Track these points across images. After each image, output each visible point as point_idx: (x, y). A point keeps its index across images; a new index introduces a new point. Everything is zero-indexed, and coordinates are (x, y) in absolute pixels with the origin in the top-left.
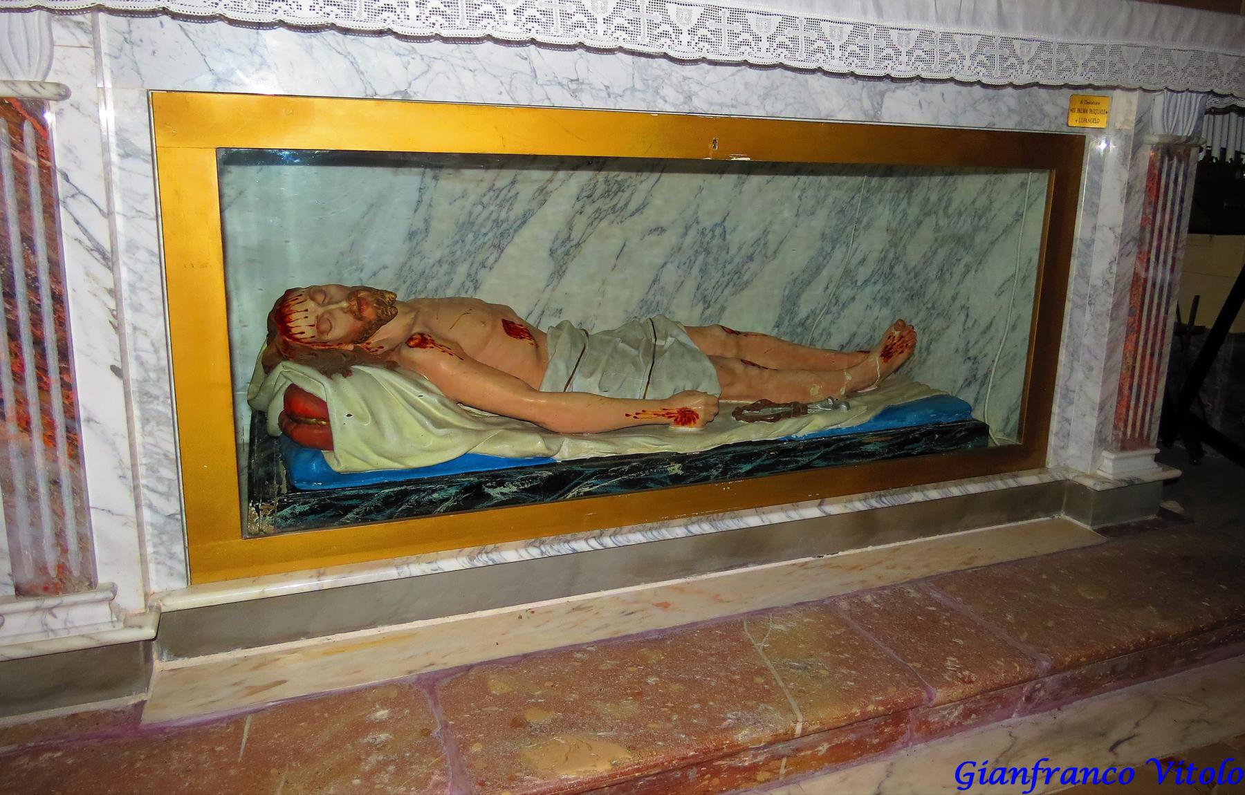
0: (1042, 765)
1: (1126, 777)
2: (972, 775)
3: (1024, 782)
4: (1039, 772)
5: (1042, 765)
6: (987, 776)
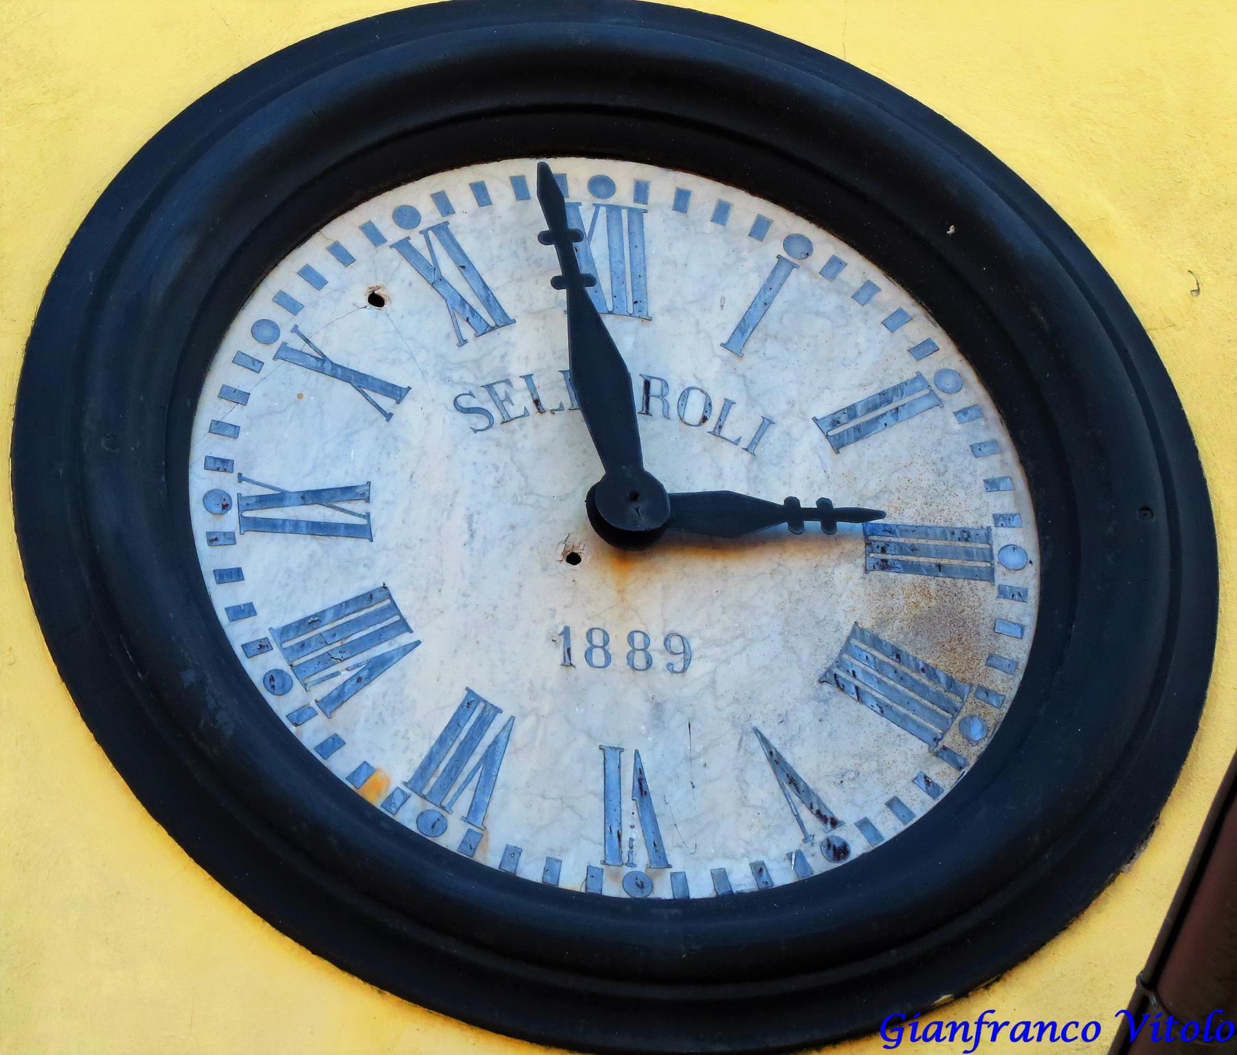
0: (989, 1018)
1: (1091, 1031)
3: (965, 1039)
4: (984, 1027)
5: (989, 1018)
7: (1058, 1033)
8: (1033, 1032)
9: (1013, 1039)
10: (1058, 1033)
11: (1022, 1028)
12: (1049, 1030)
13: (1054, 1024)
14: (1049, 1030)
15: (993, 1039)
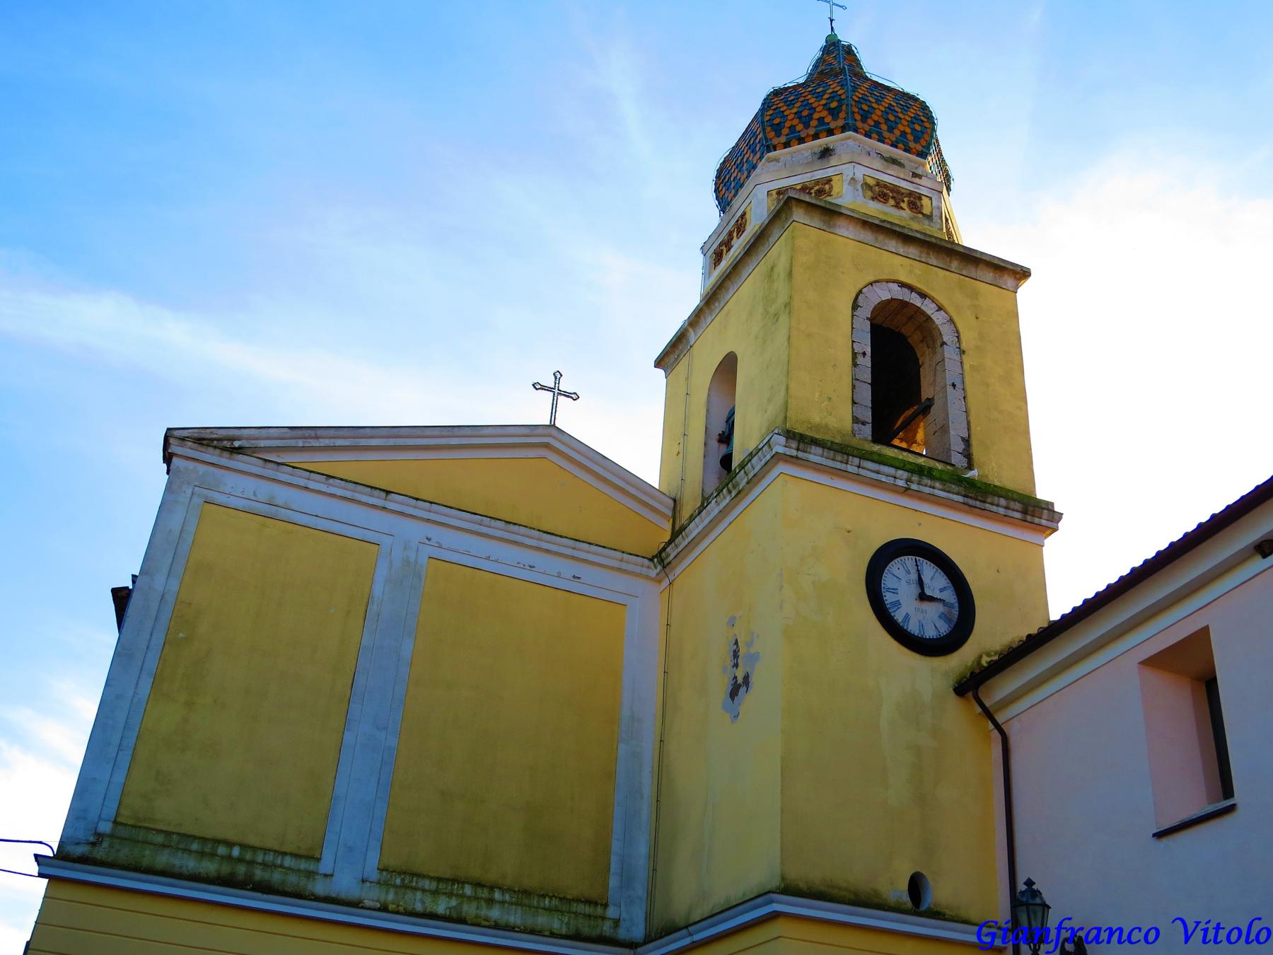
0: (1066, 924)
4: (1063, 931)
7: (1125, 937)
8: (1104, 936)
10: (1125, 937)
11: (1094, 932)
13: (1121, 929)
14: (1117, 934)
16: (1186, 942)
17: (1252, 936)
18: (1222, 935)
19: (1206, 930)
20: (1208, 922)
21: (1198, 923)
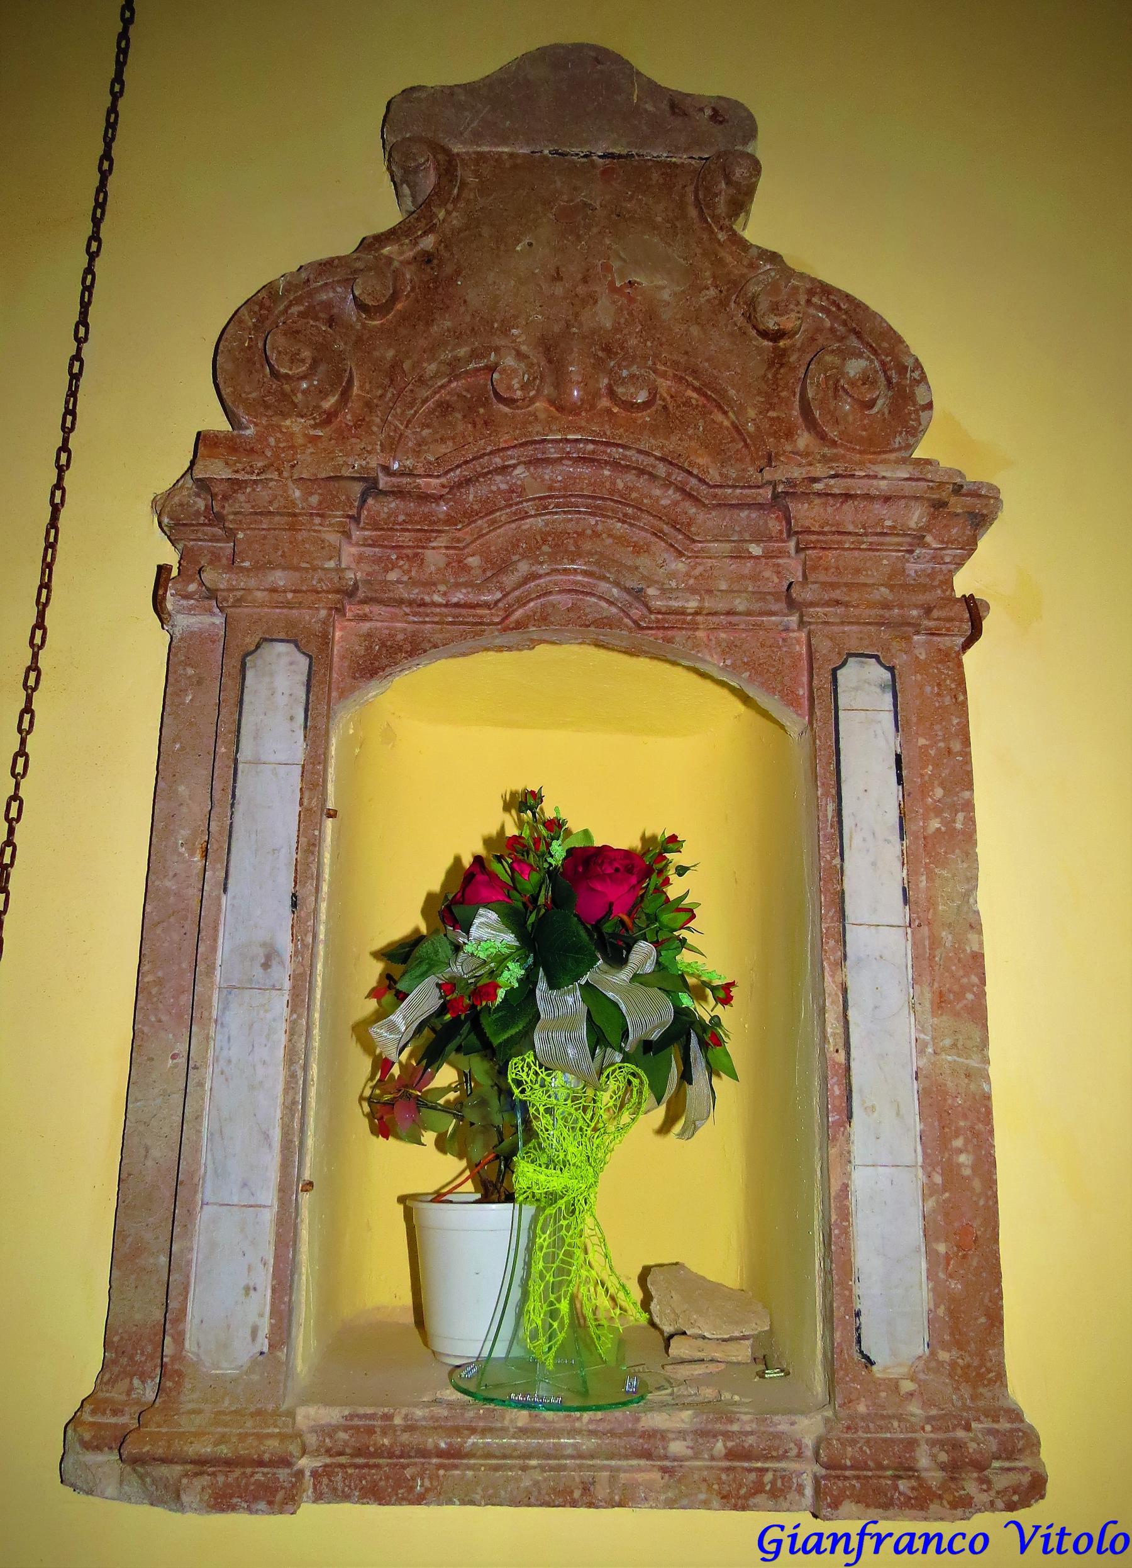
0: (871, 1529)
1: (979, 1544)
2: (779, 1542)
3: (846, 1551)
4: (867, 1538)
6: (799, 1544)
7: (944, 1545)
9: (897, 1551)
10: (944, 1545)
11: (906, 1539)
12: (934, 1542)
14: (934, 1542)
15: (876, 1551)
16: (1022, 1552)
17: (1106, 1544)
18: (1068, 1543)
19: (1047, 1537)
20: (1050, 1526)
21: (1037, 1528)
